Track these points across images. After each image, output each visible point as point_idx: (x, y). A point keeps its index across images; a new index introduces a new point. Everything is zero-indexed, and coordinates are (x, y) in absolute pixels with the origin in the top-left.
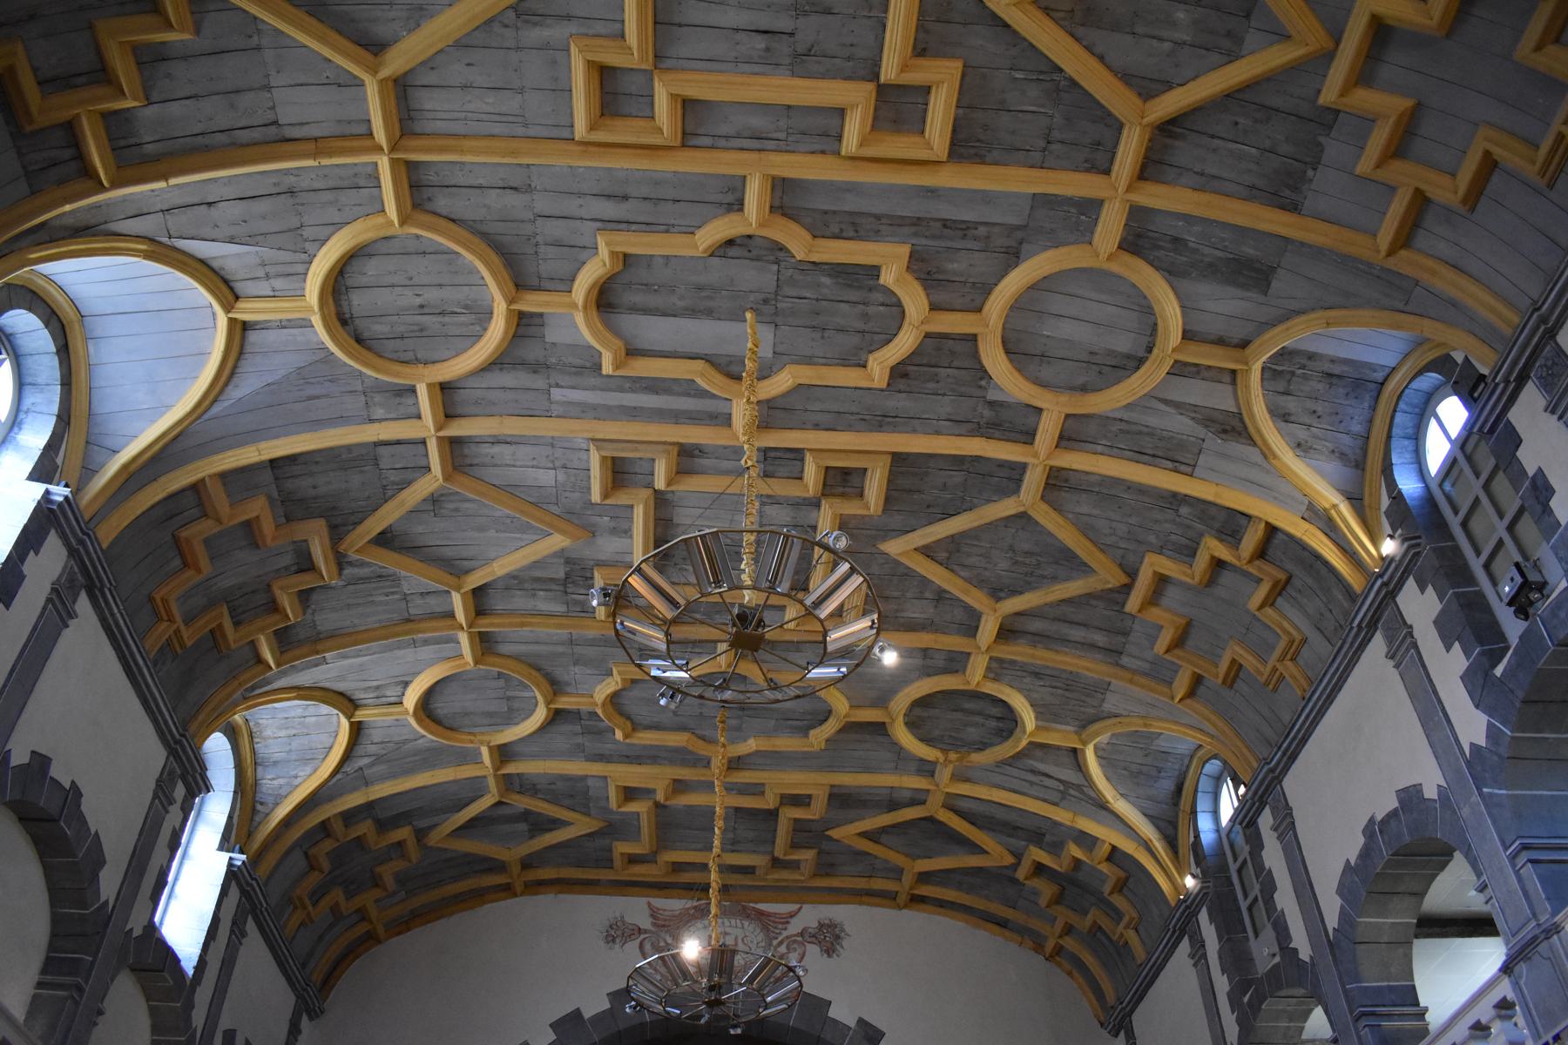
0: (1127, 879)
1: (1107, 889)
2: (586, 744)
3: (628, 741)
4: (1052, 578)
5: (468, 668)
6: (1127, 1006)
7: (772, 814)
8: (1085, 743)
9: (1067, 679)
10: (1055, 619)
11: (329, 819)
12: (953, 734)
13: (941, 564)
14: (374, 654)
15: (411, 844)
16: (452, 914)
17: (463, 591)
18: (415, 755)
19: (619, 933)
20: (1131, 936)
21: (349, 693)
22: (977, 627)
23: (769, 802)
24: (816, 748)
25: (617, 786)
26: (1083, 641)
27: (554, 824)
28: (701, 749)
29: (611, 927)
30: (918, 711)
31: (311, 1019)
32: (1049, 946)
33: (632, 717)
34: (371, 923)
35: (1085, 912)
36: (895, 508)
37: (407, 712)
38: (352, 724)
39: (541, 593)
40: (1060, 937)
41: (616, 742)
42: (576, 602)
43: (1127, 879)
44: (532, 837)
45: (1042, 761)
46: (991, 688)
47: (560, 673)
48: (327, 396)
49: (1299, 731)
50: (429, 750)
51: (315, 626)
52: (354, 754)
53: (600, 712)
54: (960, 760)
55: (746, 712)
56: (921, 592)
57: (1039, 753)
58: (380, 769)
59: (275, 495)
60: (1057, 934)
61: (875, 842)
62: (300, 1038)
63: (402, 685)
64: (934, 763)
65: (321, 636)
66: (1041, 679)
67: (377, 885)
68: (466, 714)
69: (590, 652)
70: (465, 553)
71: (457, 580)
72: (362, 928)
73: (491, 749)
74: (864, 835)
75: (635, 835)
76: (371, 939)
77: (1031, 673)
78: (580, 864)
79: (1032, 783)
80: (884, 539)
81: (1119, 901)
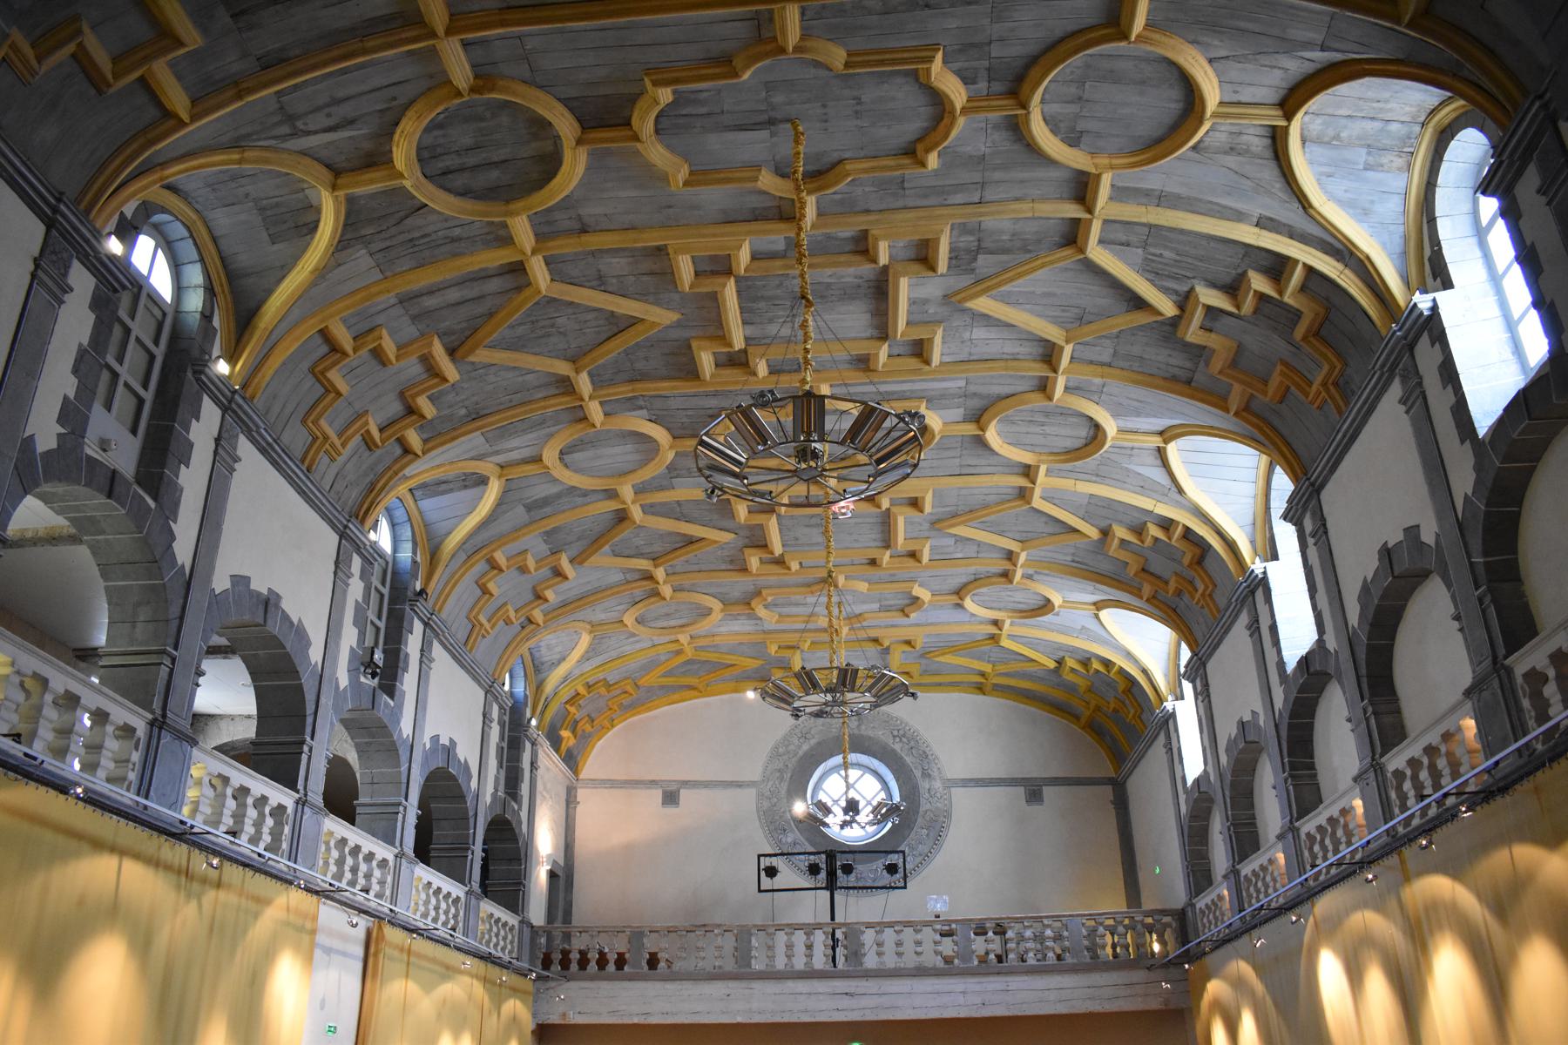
2: (986, 21)
10: (482, 297)
12: (483, 124)
14: (1211, 202)
21: (1269, 154)
26: (442, 292)
38: (1289, 117)
46: (489, 213)
48: (1128, 398)
49: (286, 463)
55: (765, 117)
57: (367, 146)
59: (1202, 364)
80: (679, 321)
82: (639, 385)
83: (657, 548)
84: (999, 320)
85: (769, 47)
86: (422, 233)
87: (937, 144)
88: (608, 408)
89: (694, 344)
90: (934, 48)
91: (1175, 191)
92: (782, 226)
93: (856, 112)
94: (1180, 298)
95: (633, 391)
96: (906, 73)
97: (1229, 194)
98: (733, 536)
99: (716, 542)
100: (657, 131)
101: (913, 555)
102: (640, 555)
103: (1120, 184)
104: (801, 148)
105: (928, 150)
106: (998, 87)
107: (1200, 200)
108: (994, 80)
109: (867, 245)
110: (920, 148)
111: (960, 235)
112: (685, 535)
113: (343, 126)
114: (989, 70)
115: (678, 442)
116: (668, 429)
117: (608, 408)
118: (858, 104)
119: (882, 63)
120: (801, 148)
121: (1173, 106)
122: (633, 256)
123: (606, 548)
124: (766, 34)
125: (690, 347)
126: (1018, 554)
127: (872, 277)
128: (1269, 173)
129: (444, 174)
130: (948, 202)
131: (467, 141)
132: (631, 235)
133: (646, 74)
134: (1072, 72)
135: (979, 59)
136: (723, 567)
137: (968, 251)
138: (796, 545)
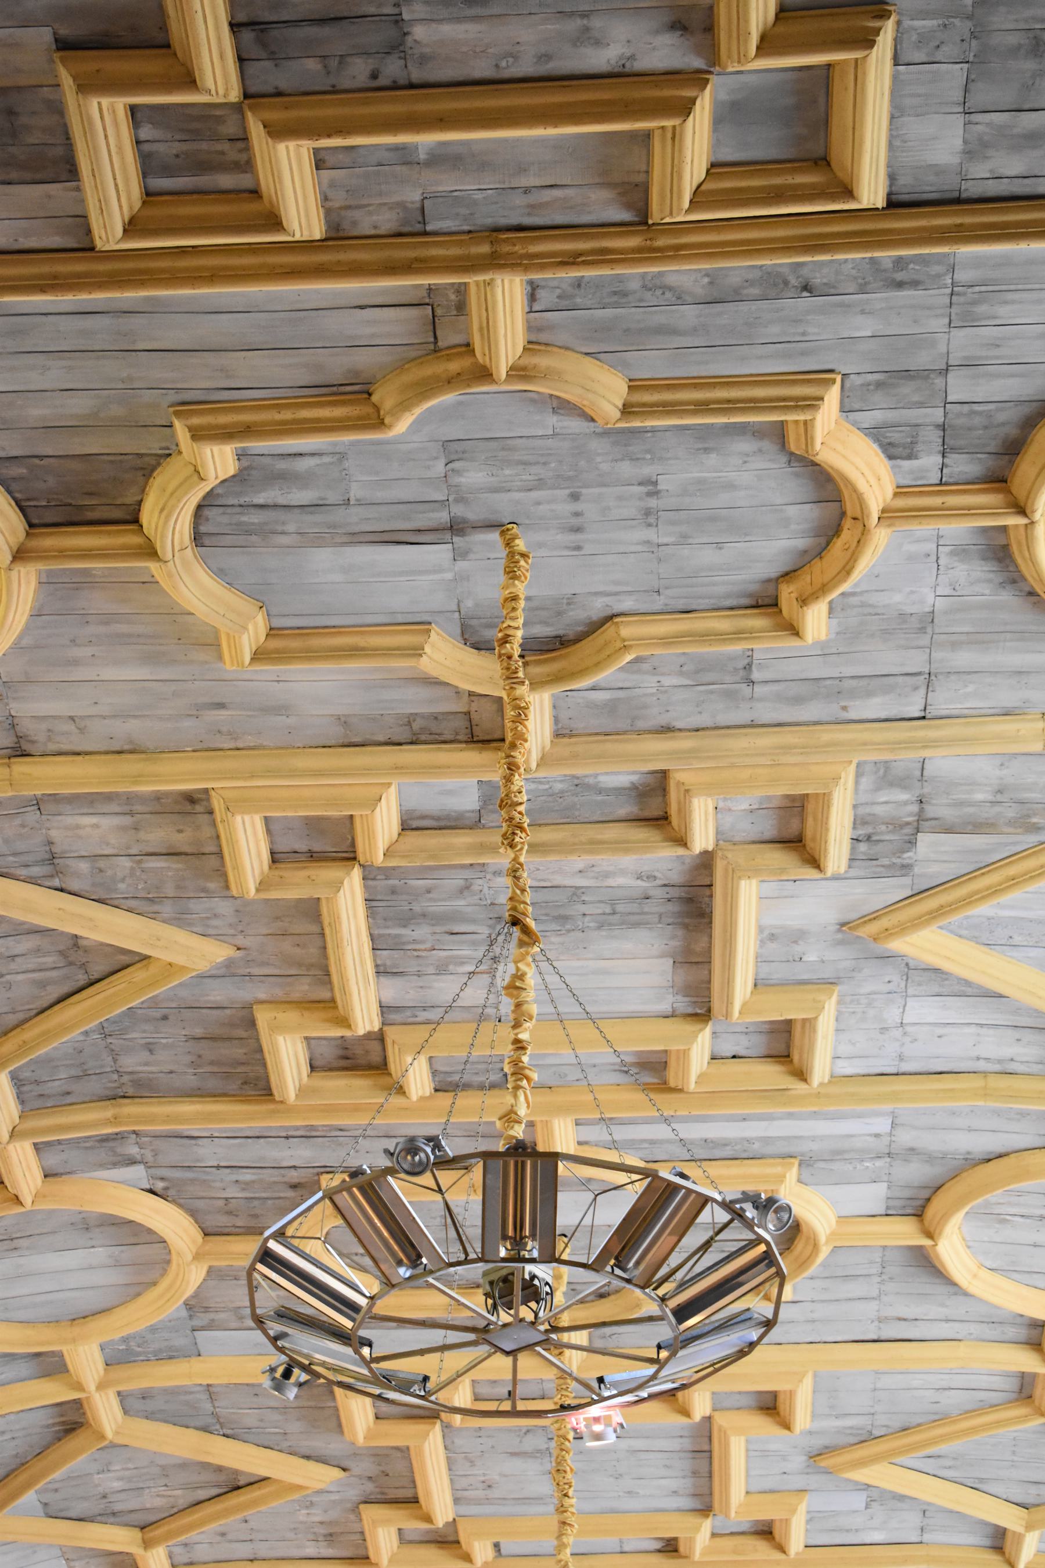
36: (228, 1012)
55: (442, 517)
80: (229, 963)
82: (130, 1109)
83: (153, 1500)
84: (968, 983)
85: (454, 366)
87: (824, 589)
88: (53, 1160)
89: (263, 1017)
90: (822, 376)
92: (471, 756)
93: (648, 512)
95: (116, 1120)
96: (757, 432)
98: (337, 1474)
99: (300, 1487)
100: (198, 538)
101: (765, 1532)
102: (110, 1516)
104: (521, 588)
105: (804, 601)
106: (963, 466)
108: (954, 449)
109: (666, 803)
110: (787, 593)
111: (878, 789)
112: (220, 1469)
114: (943, 427)
115: (218, 1244)
116: (193, 1213)
117: (53, 1160)
118: (650, 494)
119: (703, 407)
120: (521, 588)
122: (131, 814)
123: (30, 1497)
124: (448, 338)
125: (252, 1023)
126: (1019, 1538)
127: (675, 877)
130: (852, 715)
132: (130, 765)
133: (177, 414)
135: (921, 405)
136: (311, 1550)
137: (898, 826)
138: (488, 1501)
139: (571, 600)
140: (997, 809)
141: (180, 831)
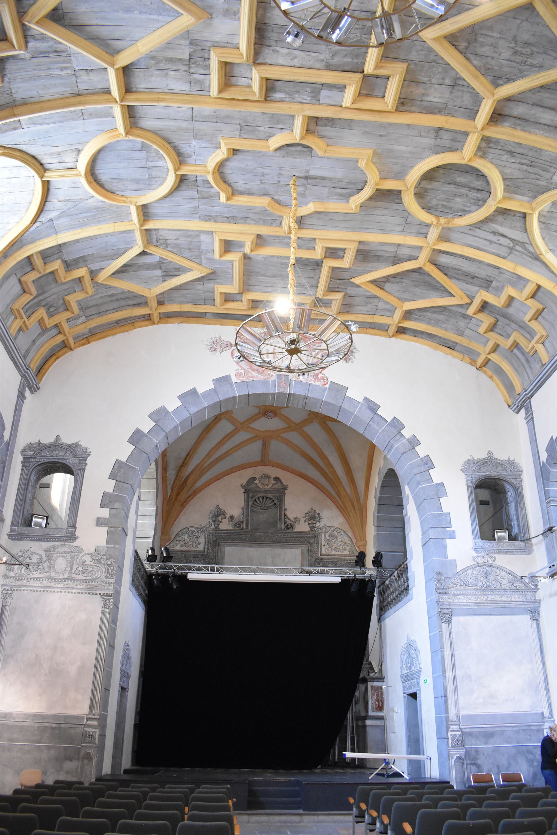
0: (543, 309)
1: (527, 318)
2: (201, 207)
3: (229, 202)
4: (540, 67)
5: (121, 138)
6: (529, 393)
7: (318, 264)
8: (533, 210)
9: (533, 157)
10: (535, 105)
11: (32, 255)
12: (445, 203)
13: (461, 53)
15: (87, 280)
16: (115, 334)
17: (116, 67)
18: (87, 212)
19: (219, 346)
20: (540, 348)
21: (39, 157)
22: (477, 111)
23: (318, 254)
24: (353, 211)
25: (220, 240)
27: (179, 270)
28: (277, 211)
29: (213, 342)
30: (425, 184)
31: (32, 392)
32: (480, 361)
33: (232, 184)
34: (65, 335)
35: (509, 336)
37: (80, 175)
38: (43, 182)
39: (172, 73)
40: (489, 354)
41: (220, 205)
42: (198, 82)
43: (543, 309)
44: (164, 281)
45: (501, 225)
46: (480, 164)
47: (186, 148)
50: (97, 208)
51: (11, 94)
52: (46, 208)
53: (210, 178)
54: (448, 222)
55: (309, 181)
56: (443, 78)
57: (500, 218)
58: (64, 221)
60: (487, 352)
61: (381, 288)
62: (25, 401)
63: (76, 153)
64: (429, 226)
65: (17, 103)
66: (513, 156)
67: (68, 310)
68: (121, 180)
69: (204, 127)
70: (118, 33)
71: (111, 57)
72: (60, 338)
73: (137, 207)
74: (373, 282)
75: (230, 280)
76: (65, 346)
77: (508, 151)
78: (193, 302)
79: (491, 242)
81: (534, 325)
86: (521, 166)
91: (75, 122)
93: (263, 176)
94: (30, 33)
97: (46, 132)
100: (366, 182)
103: (110, 119)
107: (60, 122)
109: (267, 84)
111: (203, 80)
113: (498, 233)
118: (262, 180)
121: (100, 171)
128: (32, 150)
129: (482, 190)
131: (458, 199)
134: (156, 182)
135: (203, 191)
139: (284, 156)
140: (166, 67)
141: (412, 92)
